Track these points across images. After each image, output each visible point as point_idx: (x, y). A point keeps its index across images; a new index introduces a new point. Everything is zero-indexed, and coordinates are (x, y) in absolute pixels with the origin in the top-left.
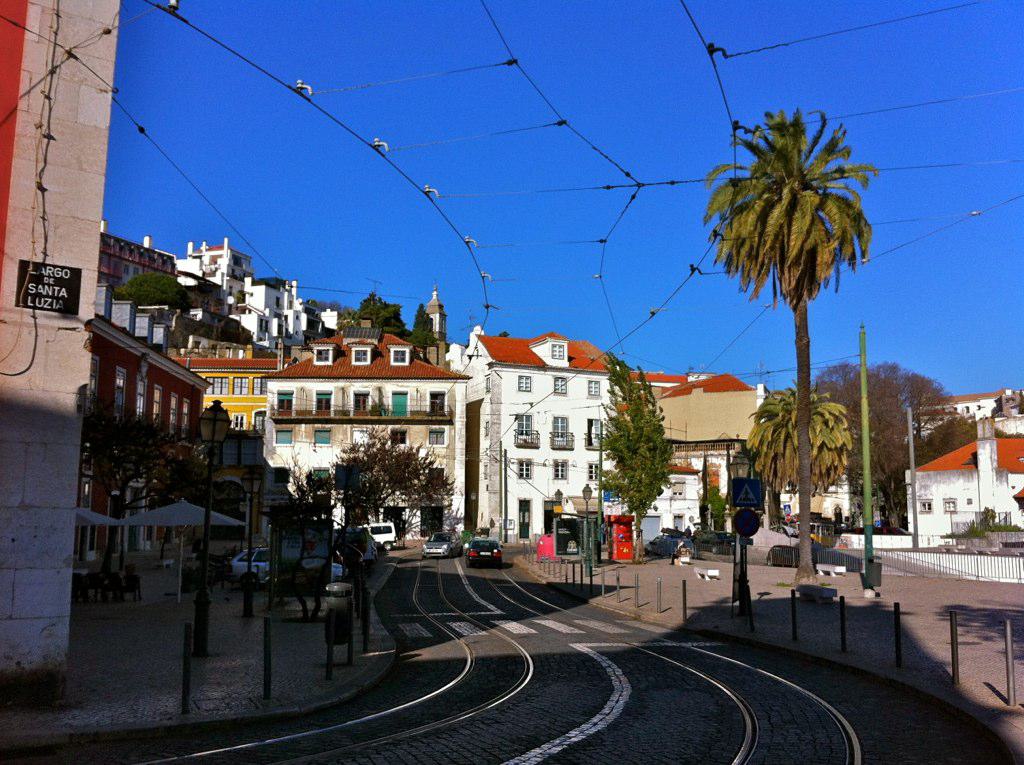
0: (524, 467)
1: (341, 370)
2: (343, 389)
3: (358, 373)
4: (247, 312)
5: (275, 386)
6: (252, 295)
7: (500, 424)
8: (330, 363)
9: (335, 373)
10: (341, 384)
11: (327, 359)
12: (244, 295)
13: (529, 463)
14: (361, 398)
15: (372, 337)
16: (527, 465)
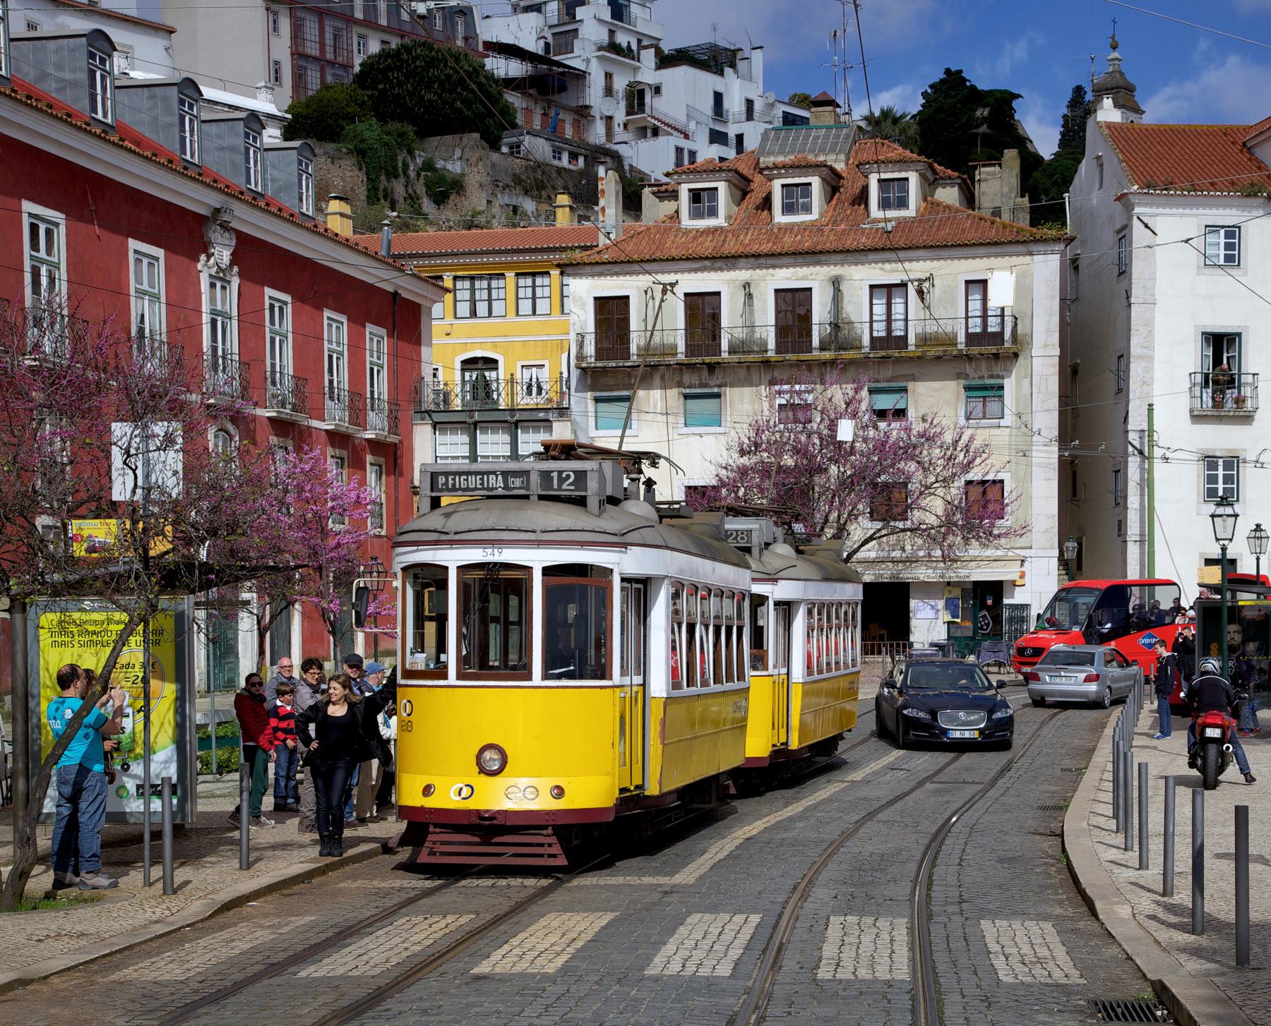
0: (1221, 472)
1: (749, 241)
2: (747, 285)
3: (788, 242)
4: (649, 132)
5: (584, 291)
6: (657, 90)
7: (1152, 357)
8: (720, 221)
9: (731, 247)
10: (743, 275)
11: (713, 212)
12: (641, 94)
13: (1232, 462)
14: (794, 306)
15: (832, 150)
16: (1228, 465)
